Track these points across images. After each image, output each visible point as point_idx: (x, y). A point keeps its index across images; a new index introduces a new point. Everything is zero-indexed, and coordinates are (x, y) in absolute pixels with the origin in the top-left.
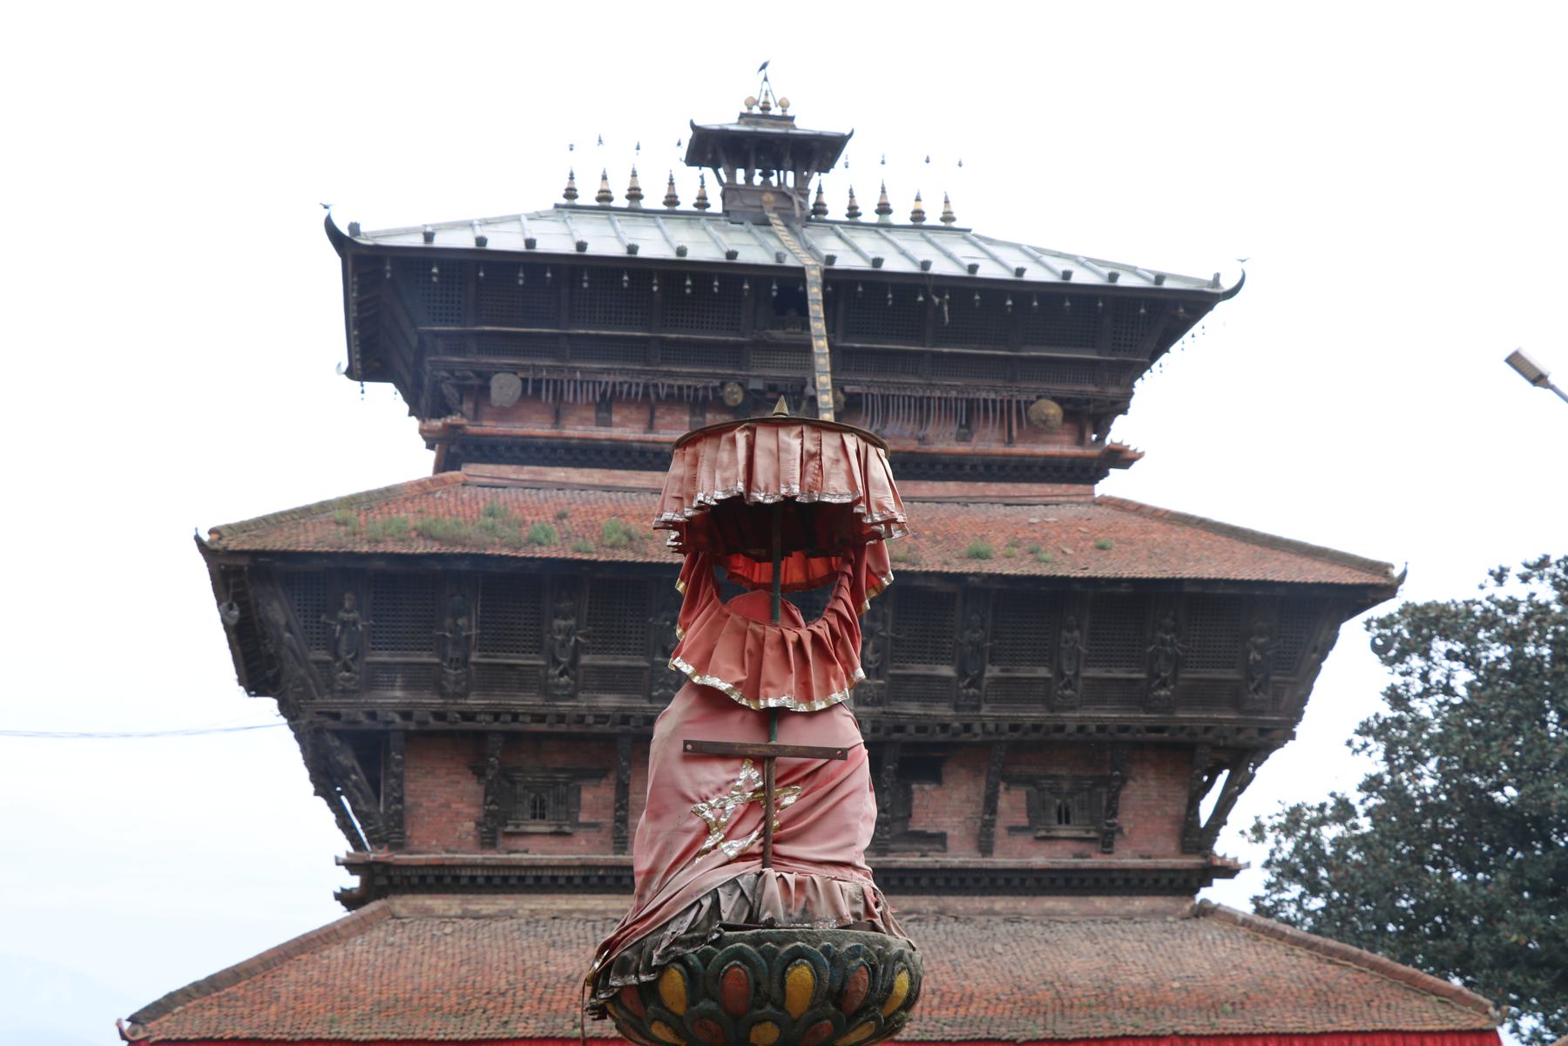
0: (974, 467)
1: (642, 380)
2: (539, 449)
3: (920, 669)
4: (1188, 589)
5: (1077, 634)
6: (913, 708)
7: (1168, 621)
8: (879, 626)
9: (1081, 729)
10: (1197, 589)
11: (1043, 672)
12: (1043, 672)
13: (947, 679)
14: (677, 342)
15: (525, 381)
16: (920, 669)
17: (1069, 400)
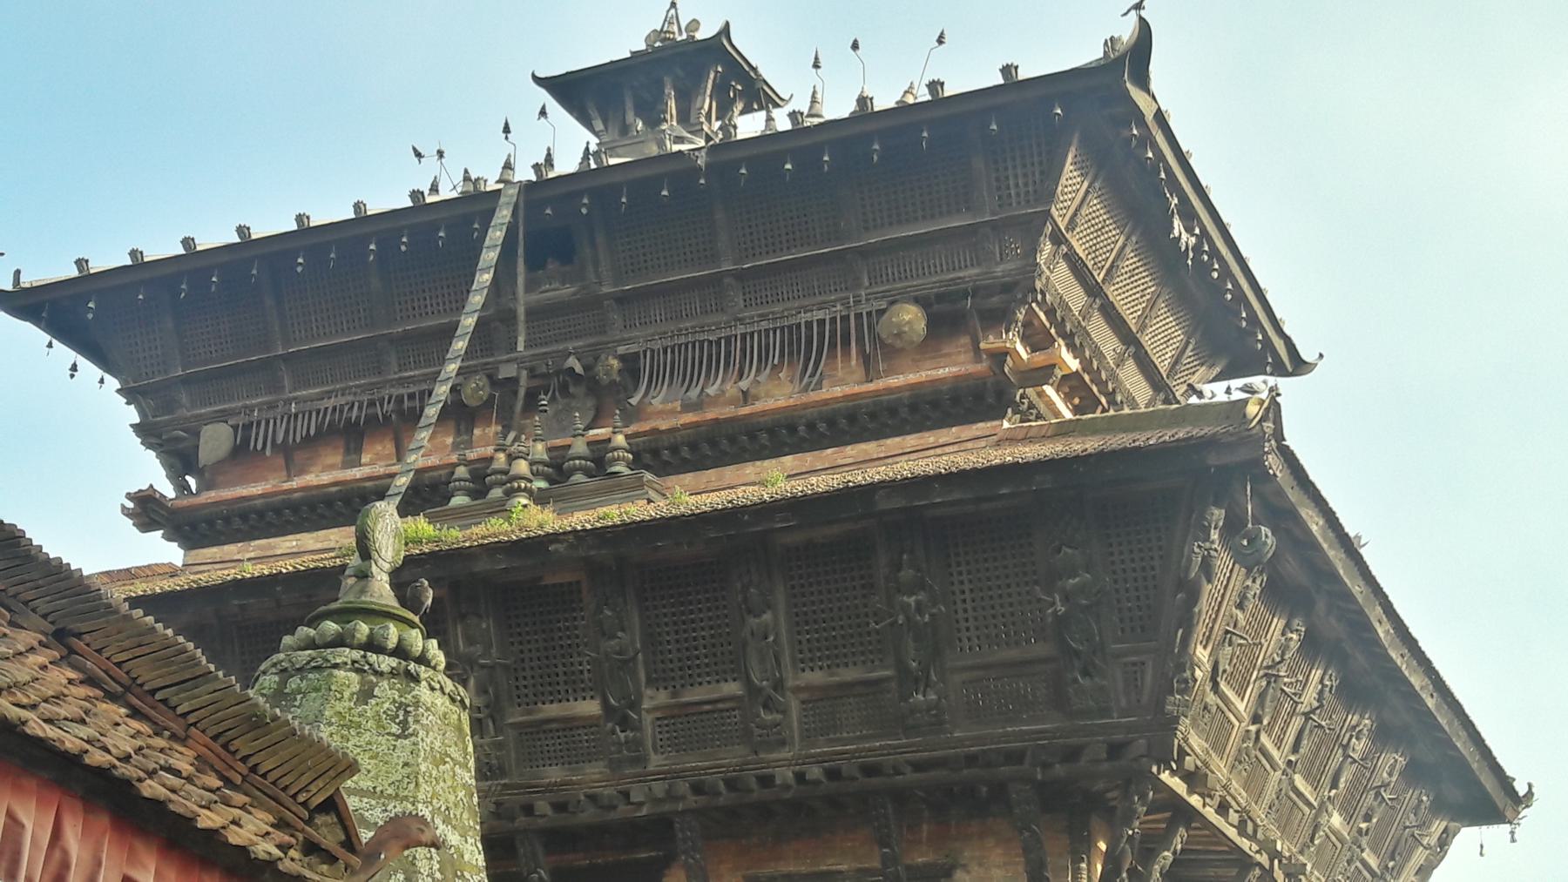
0: (811, 426)
1: (365, 398)
2: (261, 514)
3: (552, 710)
4: (884, 504)
5: (767, 617)
6: (554, 774)
7: (907, 574)
8: (478, 649)
9: (800, 777)
10: (898, 503)
11: (732, 688)
12: (732, 688)
13: (588, 723)
14: (406, 337)
15: (235, 428)
16: (552, 710)
17: (940, 298)
